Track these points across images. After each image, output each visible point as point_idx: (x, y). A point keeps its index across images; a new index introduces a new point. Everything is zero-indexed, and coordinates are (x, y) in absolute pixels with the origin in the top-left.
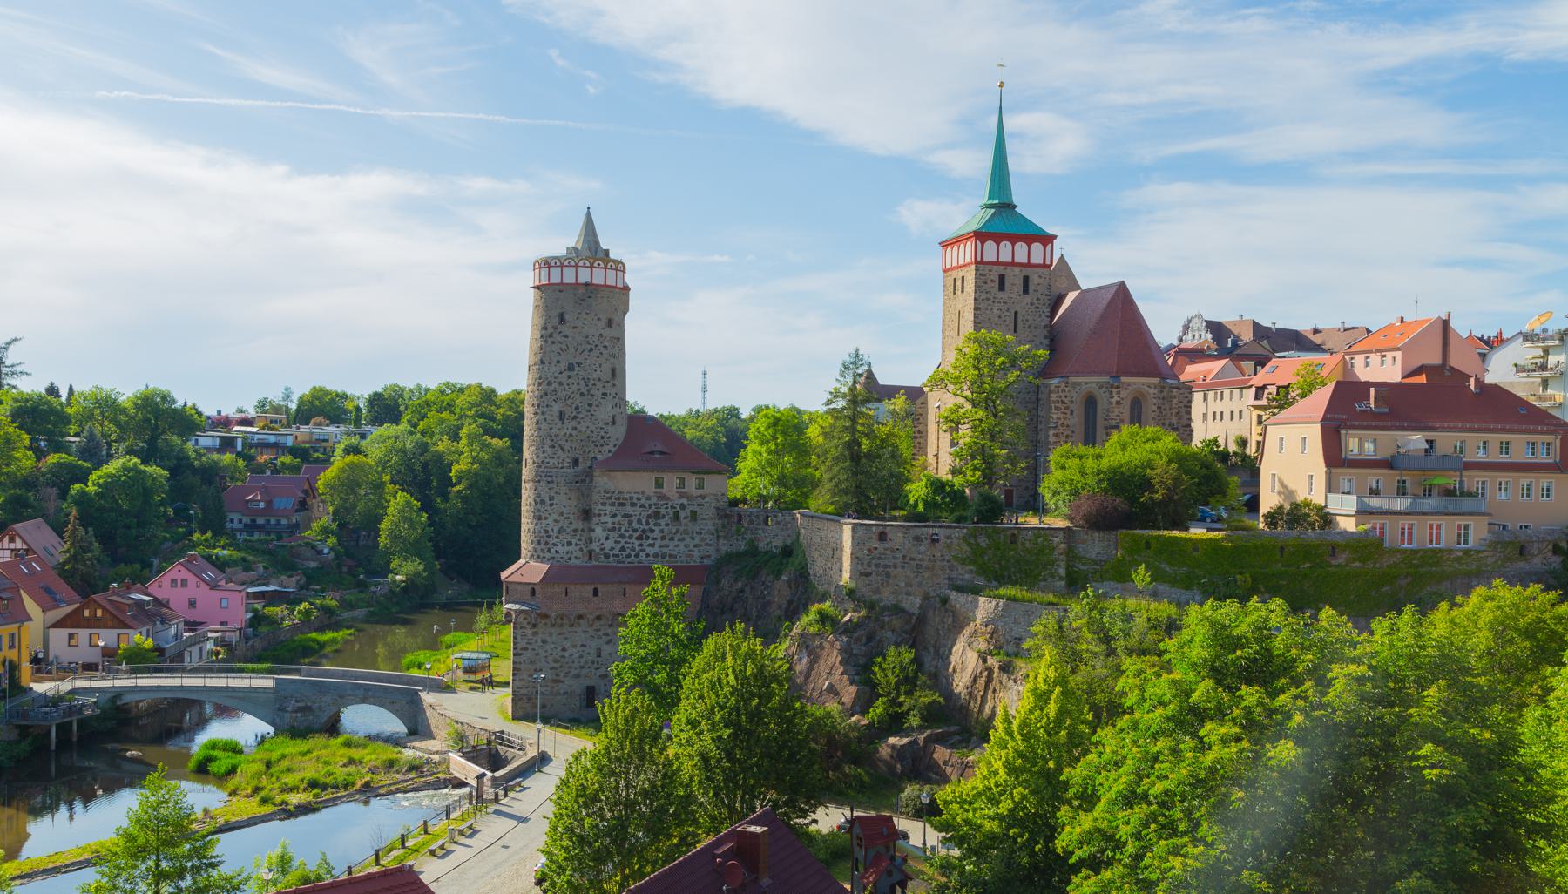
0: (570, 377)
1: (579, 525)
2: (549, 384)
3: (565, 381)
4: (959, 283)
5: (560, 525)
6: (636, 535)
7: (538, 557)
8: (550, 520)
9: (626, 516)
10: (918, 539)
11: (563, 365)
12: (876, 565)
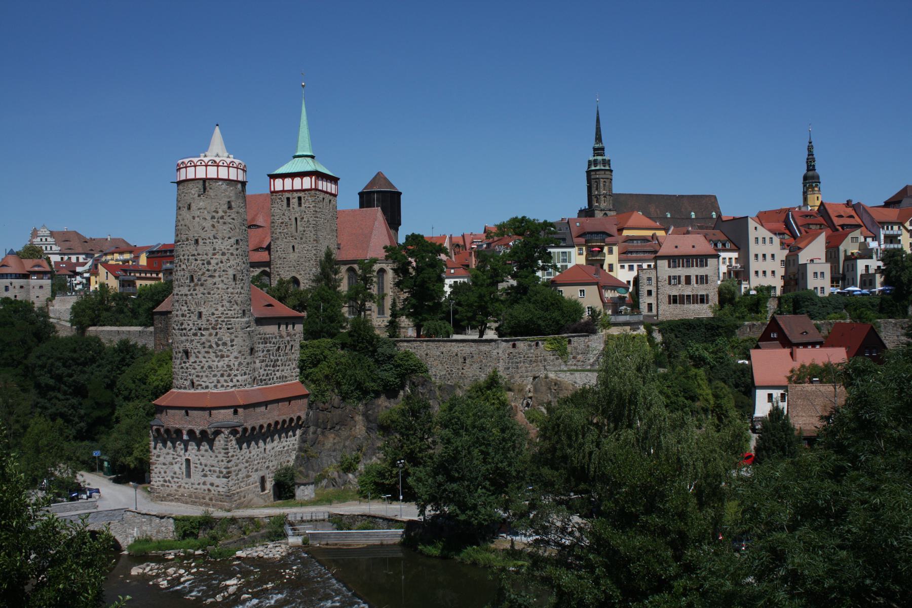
0: (237, 249)
1: (249, 359)
2: (224, 254)
3: (235, 253)
4: (294, 201)
5: (239, 360)
6: (272, 363)
7: (222, 386)
9: (268, 351)
11: (233, 240)
12: (512, 363)
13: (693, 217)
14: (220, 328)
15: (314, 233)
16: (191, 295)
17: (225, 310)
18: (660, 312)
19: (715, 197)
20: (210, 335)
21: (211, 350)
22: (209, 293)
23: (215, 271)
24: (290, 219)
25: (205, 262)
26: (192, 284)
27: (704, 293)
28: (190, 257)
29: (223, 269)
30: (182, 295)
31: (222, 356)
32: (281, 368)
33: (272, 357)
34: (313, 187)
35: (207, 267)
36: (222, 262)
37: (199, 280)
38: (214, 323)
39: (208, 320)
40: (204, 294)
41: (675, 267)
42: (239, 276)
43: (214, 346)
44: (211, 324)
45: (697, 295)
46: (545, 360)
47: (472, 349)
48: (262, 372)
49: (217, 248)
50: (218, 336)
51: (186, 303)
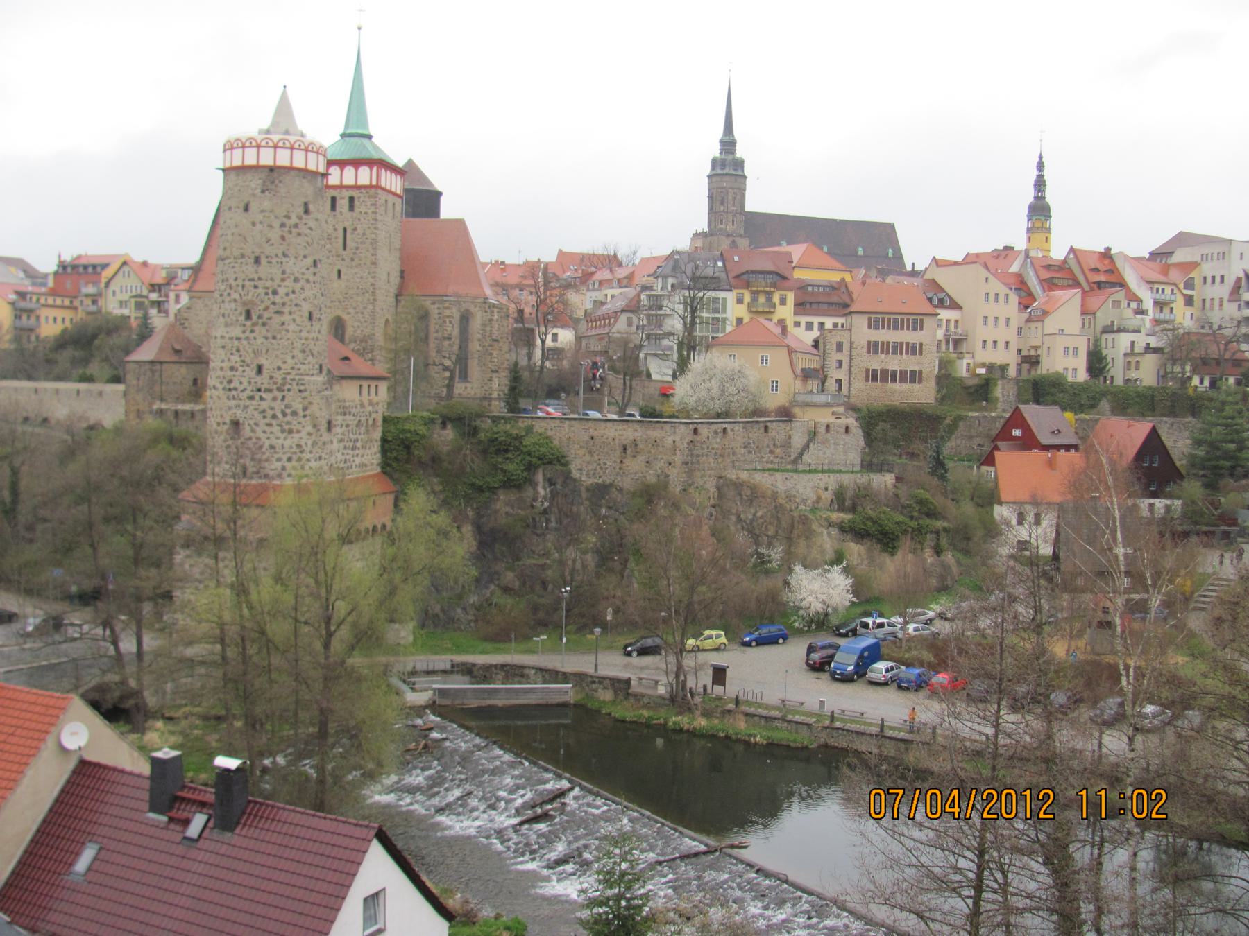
0: (315, 274)
1: (326, 437)
2: (296, 280)
3: (312, 278)
4: (343, 204)
6: (351, 444)
8: (304, 434)
9: (347, 426)
10: (716, 432)
11: (309, 261)
13: (861, 252)
14: (289, 390)
15: (372, 252)
16: (247, 338)
17: (296, 364)
18: (853, 392)
19: (891, 227)
20: (275, 399)
21: (274, 422)
22: (274, 338)
23: (284, 304)
24: (335, 230)
25: (270, 291)
26: (249, 323)
27: (916, 368)
28: (247, 283)
29: (295, 302)
30: (231, 339)
31: (290, 432)
32: (360, 452)
33: (351, 435)
34: (374, 183)
35: (272, 299)
36: (293, 292)
37: (260, 317)
38: (280, 381)
39: (271, 378)
40: (267, 338)
41: (876, 328)
42: (316, 315)
43: (280, 415)
44: (275, 383)
45: (906, 371)
46: (734, 454)
47: (638, 434)
48: (340, 456)
49: (288, 271)
50: (286, 401)
51: (238, 350)
